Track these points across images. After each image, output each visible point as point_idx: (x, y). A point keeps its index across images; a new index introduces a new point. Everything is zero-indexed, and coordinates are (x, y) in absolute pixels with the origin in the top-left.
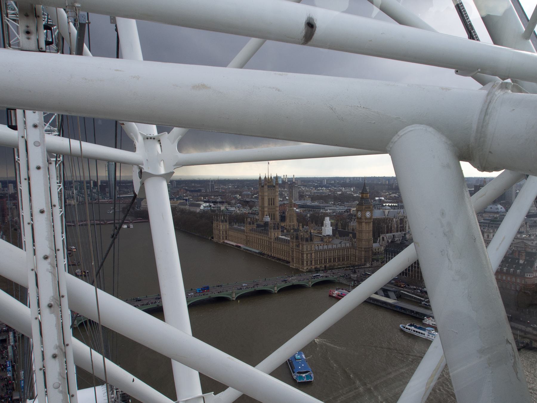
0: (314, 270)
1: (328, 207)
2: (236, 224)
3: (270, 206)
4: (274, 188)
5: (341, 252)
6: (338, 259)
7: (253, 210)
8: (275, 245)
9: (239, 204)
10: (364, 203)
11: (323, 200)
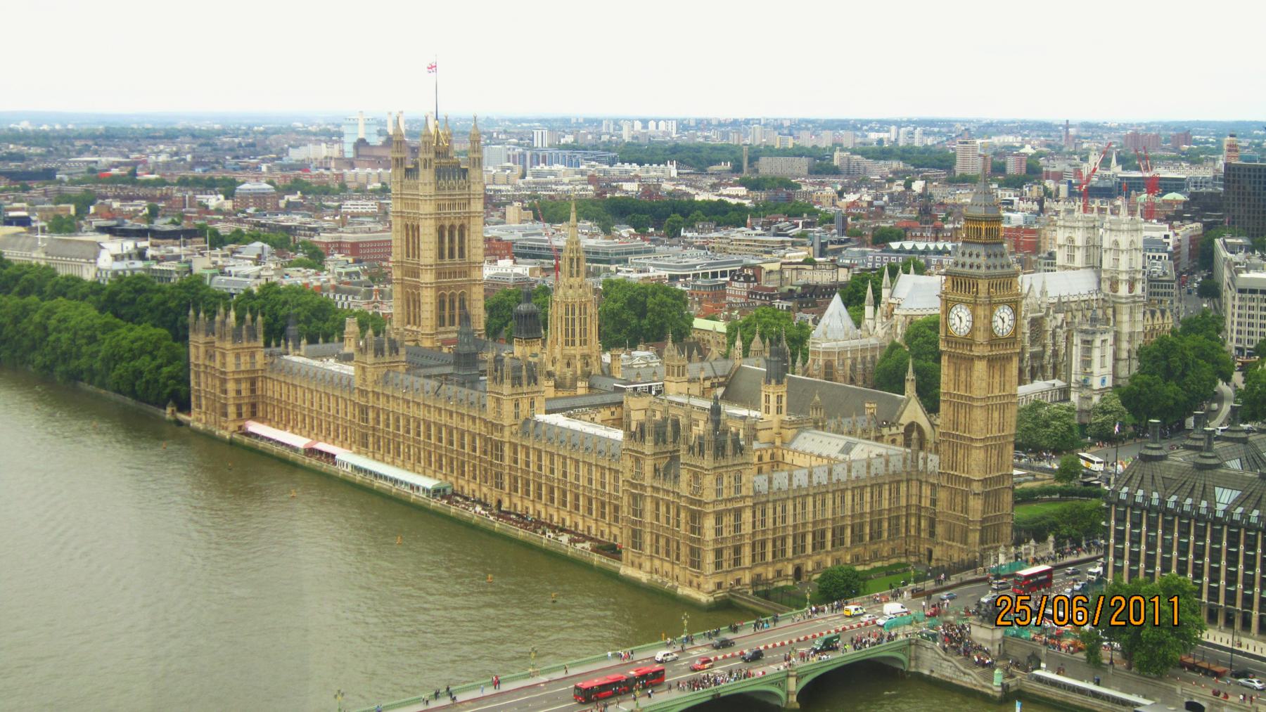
0: (751, 592)
1: (637, 253)
2: (297, 347)
3: (447, 260)
4: (462, 180)
5: (867, 497)
6: (852, 531)
7: (340, 274)
8: (521, 456)
9: (258, 244)
10: (988, 268)
11: (592, 220)
